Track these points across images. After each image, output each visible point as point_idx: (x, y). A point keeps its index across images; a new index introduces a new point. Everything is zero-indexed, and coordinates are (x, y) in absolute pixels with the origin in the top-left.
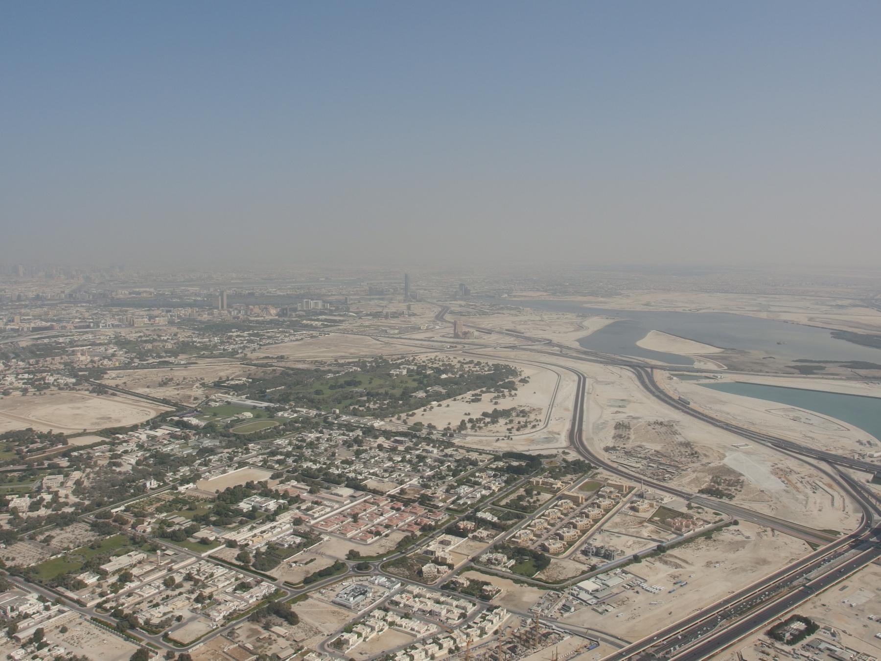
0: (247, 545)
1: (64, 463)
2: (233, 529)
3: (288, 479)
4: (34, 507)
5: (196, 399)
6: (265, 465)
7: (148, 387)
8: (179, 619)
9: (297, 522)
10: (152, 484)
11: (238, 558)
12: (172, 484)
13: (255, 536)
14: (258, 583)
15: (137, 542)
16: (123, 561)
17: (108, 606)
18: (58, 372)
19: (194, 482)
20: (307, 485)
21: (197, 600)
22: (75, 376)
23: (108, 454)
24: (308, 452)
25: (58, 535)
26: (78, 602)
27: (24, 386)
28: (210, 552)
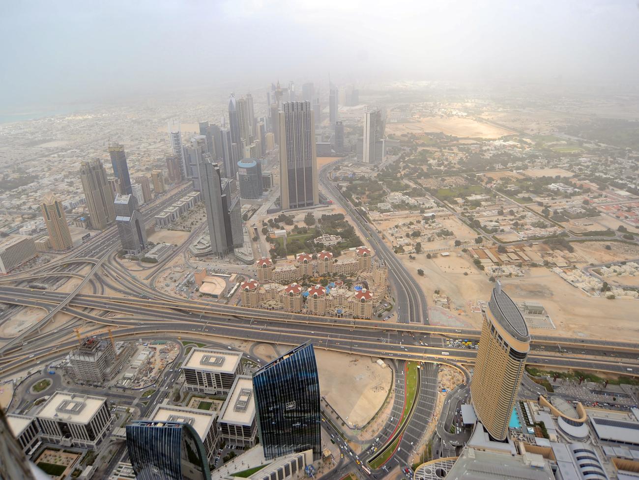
0: (550, 206)
1: (456, 150)
2: (542, 197)
3: (584, 179)
4: (439, 165)
5: (532, 130)
6: (570, 169)
7: (505, 122)
8: (502, 231)
9: (586, 202)
10: (499, 166)
11: (543, 212)
12: (510, 168)
13: (556, 203)
14: (552, 226)
15: (488, 191)
16: (479, 197)
17: (467, 215)
18: (459, 109)
19: (524, 170)
20: (597, 185)
21: (514, 224)
22: (468, 112)
23: (478, 150)
24: (601, 168)
25: (448, 179)
26: (453, 209)
27: (442, 114)
28: (526, 205)
